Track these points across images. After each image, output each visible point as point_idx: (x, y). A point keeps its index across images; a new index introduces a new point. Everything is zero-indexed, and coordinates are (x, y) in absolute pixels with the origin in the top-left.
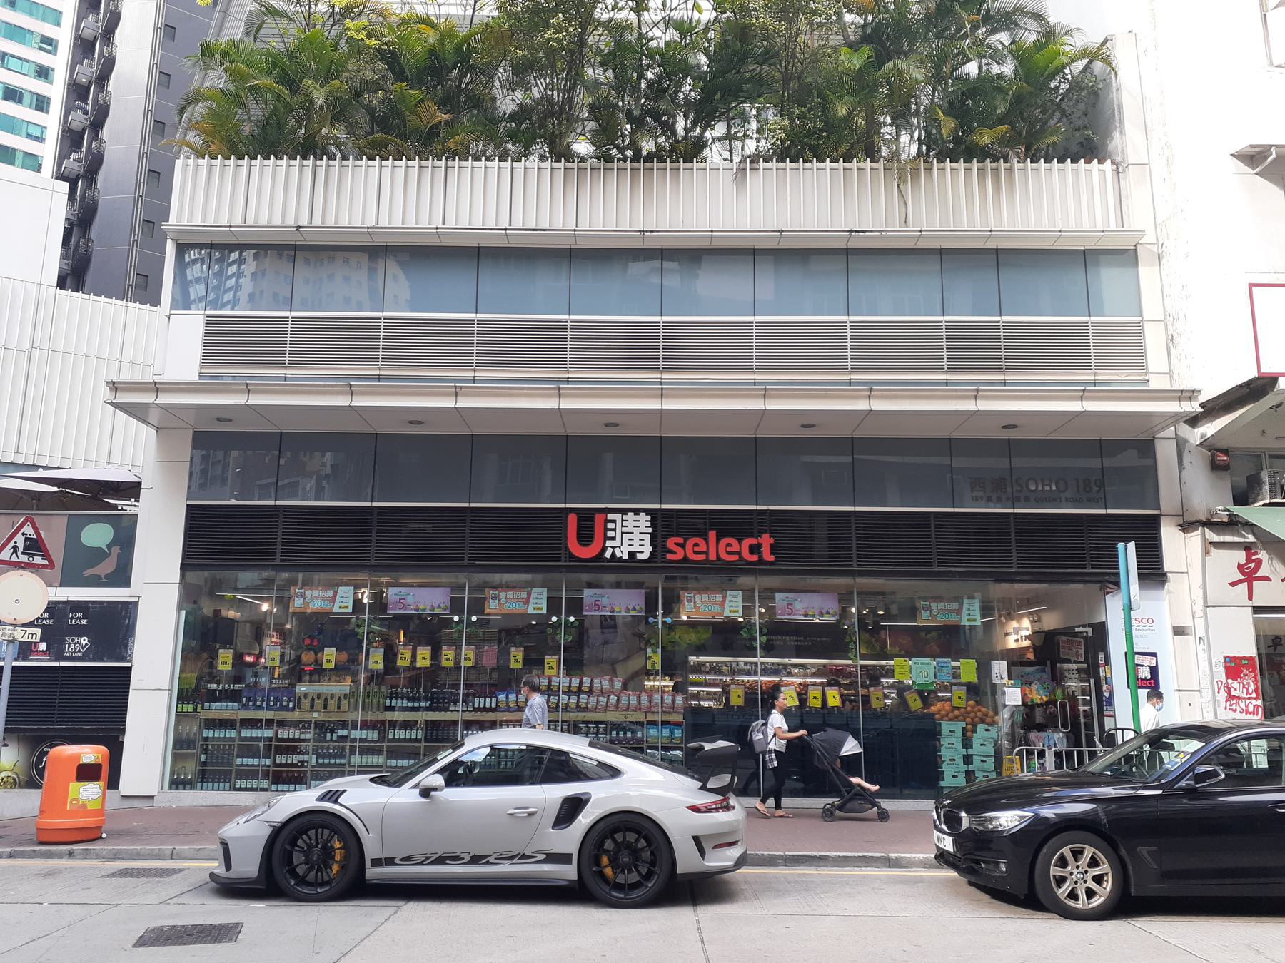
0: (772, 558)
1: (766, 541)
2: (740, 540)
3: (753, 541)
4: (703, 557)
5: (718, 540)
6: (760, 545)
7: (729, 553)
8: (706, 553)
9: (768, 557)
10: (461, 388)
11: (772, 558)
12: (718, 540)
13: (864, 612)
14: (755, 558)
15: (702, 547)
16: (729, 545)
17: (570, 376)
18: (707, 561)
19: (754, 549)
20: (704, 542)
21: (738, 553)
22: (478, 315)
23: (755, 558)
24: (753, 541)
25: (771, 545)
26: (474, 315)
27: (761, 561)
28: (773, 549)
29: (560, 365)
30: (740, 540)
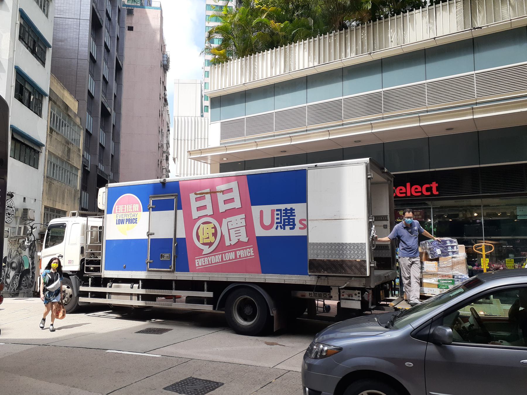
0: (437, 193)
1: (434, 185)
2: (421, 186)
3: (428, 186)
4: (404, 195)
5: (411, 187)
6: (431, 188)
7: (416, 192)
8: (406, 193)
9: (435, 192)
10: (292, 137)
11: (437, 193)
12: (411, 187)
13: (499, 214)
14: (429, 193)
15: (404, 191)
16: (416, 189)
17: (344, 123)
18: (406, 197)
19: (429, 189)
20: (405, 188)
21: (421, 192)
22: (308, 104)
23: (429, 193)
24: (428, 186)
25: (437, 187)
26: (306, 104)
27: (432, 195)
28: (438, 189)
29: (339, 118)
30: (421, 186)
